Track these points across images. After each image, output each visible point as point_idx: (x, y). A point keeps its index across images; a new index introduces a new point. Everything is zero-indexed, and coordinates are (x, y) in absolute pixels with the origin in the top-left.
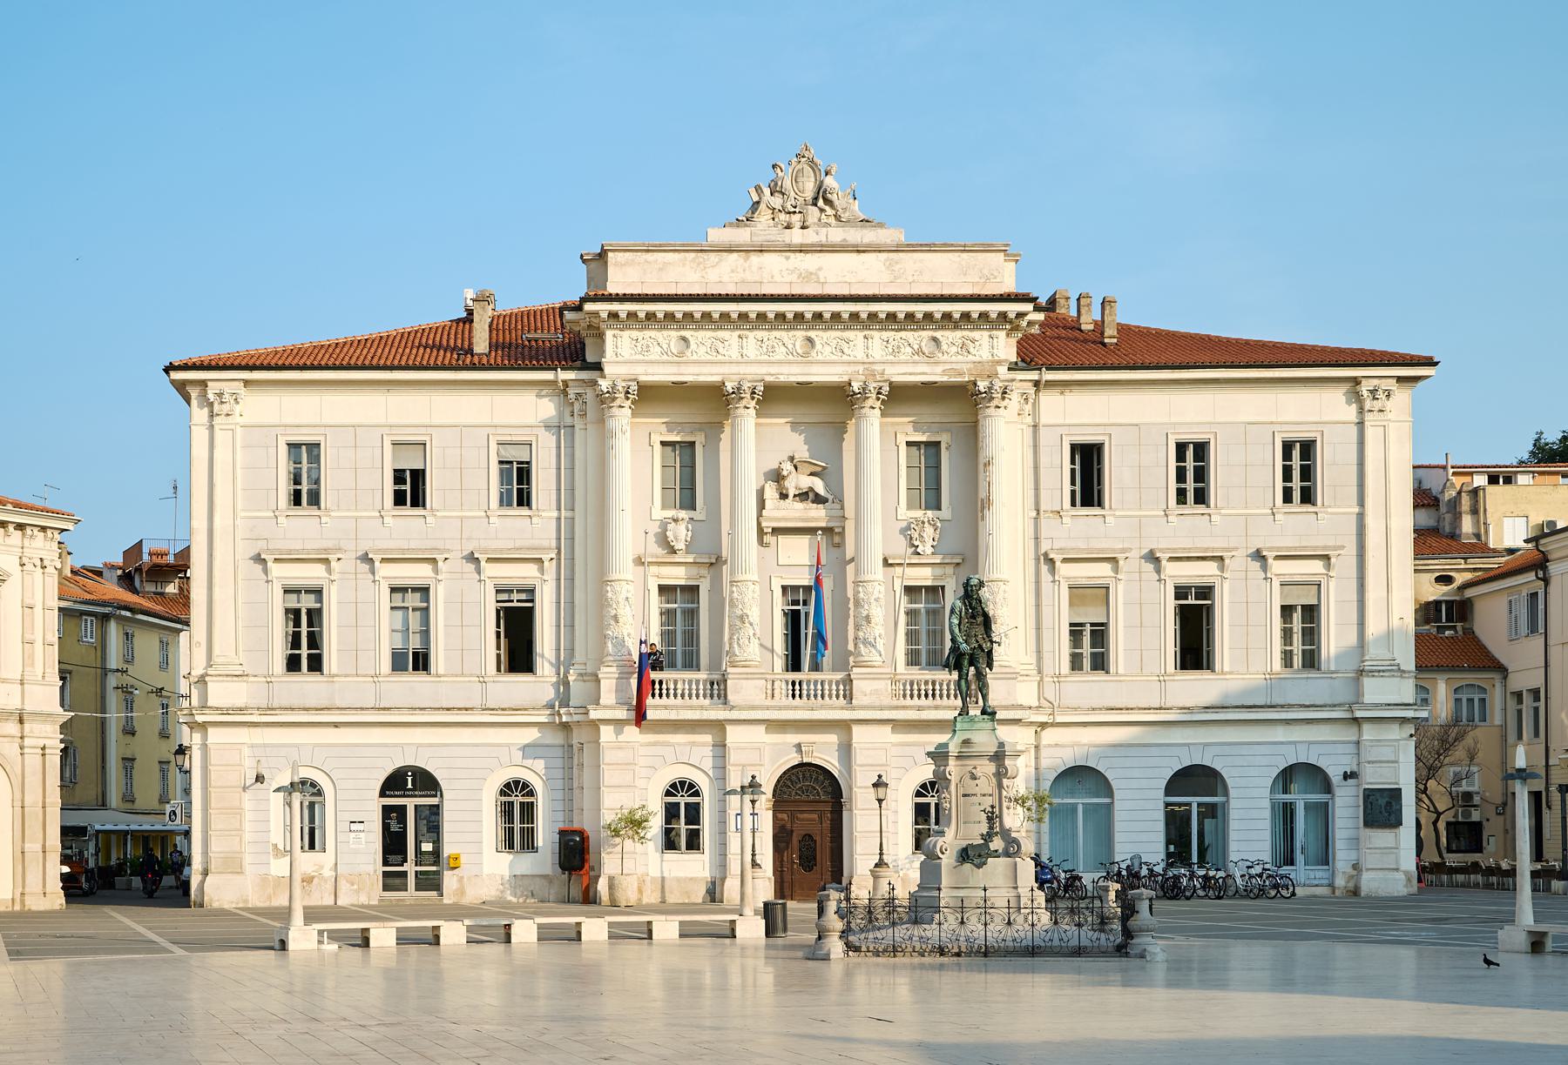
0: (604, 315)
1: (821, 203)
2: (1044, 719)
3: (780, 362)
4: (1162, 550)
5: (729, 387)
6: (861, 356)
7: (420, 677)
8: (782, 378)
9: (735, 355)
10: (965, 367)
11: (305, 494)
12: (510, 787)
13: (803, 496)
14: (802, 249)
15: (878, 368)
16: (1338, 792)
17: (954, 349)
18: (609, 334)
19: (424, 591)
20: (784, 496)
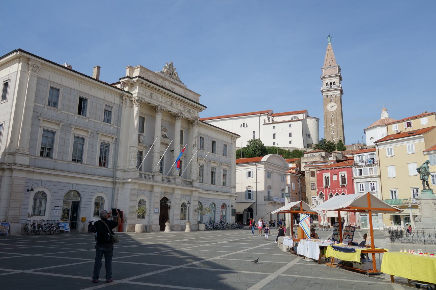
5: (160, 107)
6: (180, 108)
9: (160, 100)
11: (53, 103)
14: (173, 83)
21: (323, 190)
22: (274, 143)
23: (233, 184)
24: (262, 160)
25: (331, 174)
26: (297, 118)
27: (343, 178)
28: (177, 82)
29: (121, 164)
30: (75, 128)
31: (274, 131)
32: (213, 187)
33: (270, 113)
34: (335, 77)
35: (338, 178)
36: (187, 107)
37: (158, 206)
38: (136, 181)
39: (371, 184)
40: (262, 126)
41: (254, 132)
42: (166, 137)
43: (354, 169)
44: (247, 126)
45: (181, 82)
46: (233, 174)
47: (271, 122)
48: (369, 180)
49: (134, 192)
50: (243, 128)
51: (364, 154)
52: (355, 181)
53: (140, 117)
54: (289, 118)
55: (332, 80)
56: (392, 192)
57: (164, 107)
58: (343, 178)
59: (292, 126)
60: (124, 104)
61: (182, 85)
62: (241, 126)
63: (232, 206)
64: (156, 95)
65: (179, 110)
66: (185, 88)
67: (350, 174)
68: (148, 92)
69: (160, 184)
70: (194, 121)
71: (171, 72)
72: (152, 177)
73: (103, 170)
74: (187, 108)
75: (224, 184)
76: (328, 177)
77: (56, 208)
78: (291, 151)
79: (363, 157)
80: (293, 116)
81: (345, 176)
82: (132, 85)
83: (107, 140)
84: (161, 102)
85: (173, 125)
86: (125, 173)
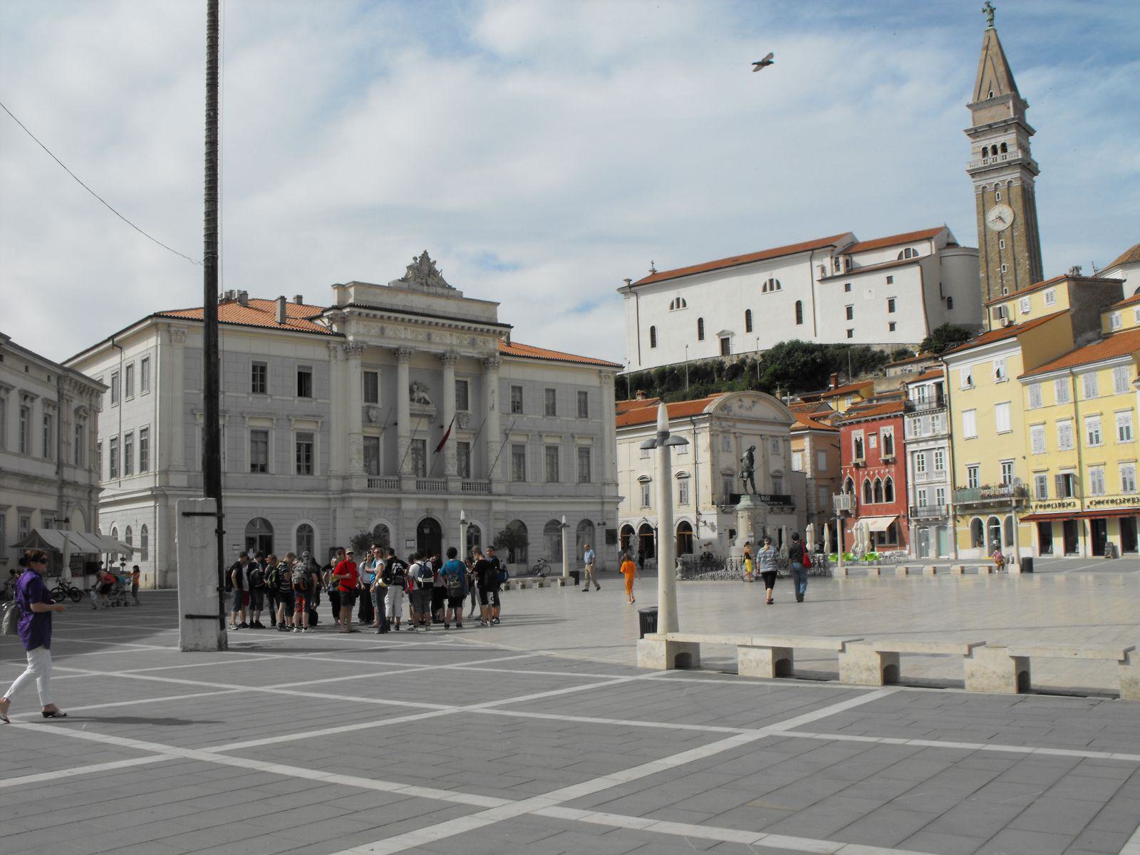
1: (432, 276)
4: (544, 432)
7: (262, 475)
9: (403, 336)
12: (303, 528)
13: (419, 401)
14: (428, 294)
15: (455, 348)
16: (597, 530)
19: (266, 433)
20: (412, 400)
21: (851, 473)
22: (850, 333)
23: (608, 476)
24: (705, 410)
25: (865, 433)
26: (915, 253)
27: (888, 441)
28: (440, 290)
29: (337, 466)
30: (250, 418)
31: (849, 298)
32: (553, 488)
33: (840, 246)
34: (1005, 126)
35: (878, 443)
36: (466, 336)
37: (414, 534)
38: (362, 495)
39: (937, 454)
40: (817, 284)
41: (799, 304)
42: (427, 403)
43: (907, 419)
44: (779, 287)
45: (450, 287)
46: (607, 453)
47: (842, 271)
48: (932, 444)
49: (360, 514)
50: (769, 294)
51: (927, 383)
52: (910, 448)
53: (366, 373)
54: (891, 255)
55: (998, 140)
56: (970, 471)
57: (412, 348)
58: (888, 441)
59: (894, 279)
60: (332, 358)
61: (451, 293)
62: (765, 289)
63: (604, 524)
64: (390, 329)
65: (445, 344)
66: (459, 297)
67: (901, 431)
68: (375, 327)
69: (415, 496)
70: (487, 359)
72: (397, 485)
73: (306, 481)
74: (467, 338)
75: (585, 478)
76: (861, 440)
77: (235, 547)
78: (888, 351)
79: (926, 389)
80: (902, 249)
81: (891, 436)
82: (344, 320)
83: (306, 427)
84: (406, 339)
85: (439, 376)
86: (346, 481)
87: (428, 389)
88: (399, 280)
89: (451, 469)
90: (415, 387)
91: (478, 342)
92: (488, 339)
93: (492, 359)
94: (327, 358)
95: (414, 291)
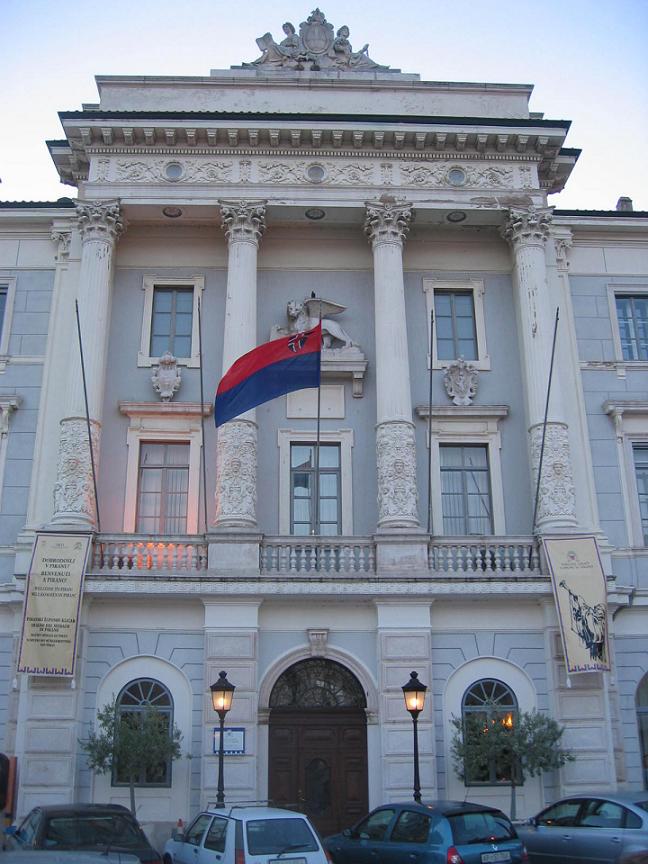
0: (85, 133)
2: (625, 600)
3: (286, 187)
6: (378, 181)
8: (288, 203)
9: (235, 178)
10: (496, 196)
15: (398, 195)
17: (482, 180)
18: (94, 162)
61: (382, 77)
65: (371, 188)
71: (313, 50)
84: (245, 185)
87: (342, 309)
88: (233, 67)
89: (392, 508)
90: (296, 307)
91: (473, 178)
92: (507, 167)
93: (516, 213)
94: (52, 263)
95: (267, 85)
